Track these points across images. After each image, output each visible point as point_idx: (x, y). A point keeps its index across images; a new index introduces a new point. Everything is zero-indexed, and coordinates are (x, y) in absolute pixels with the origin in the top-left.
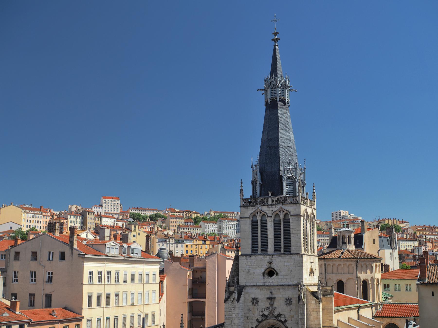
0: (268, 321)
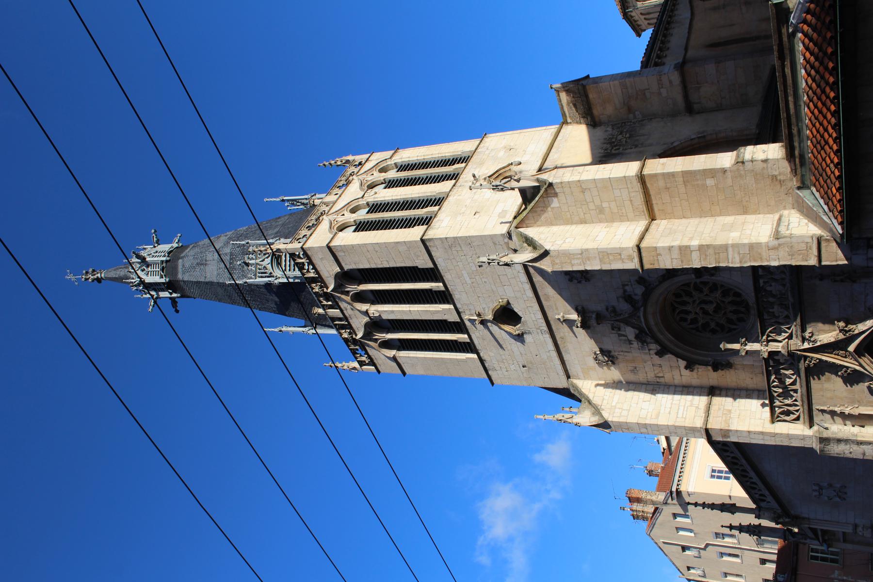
0: (655, 329)
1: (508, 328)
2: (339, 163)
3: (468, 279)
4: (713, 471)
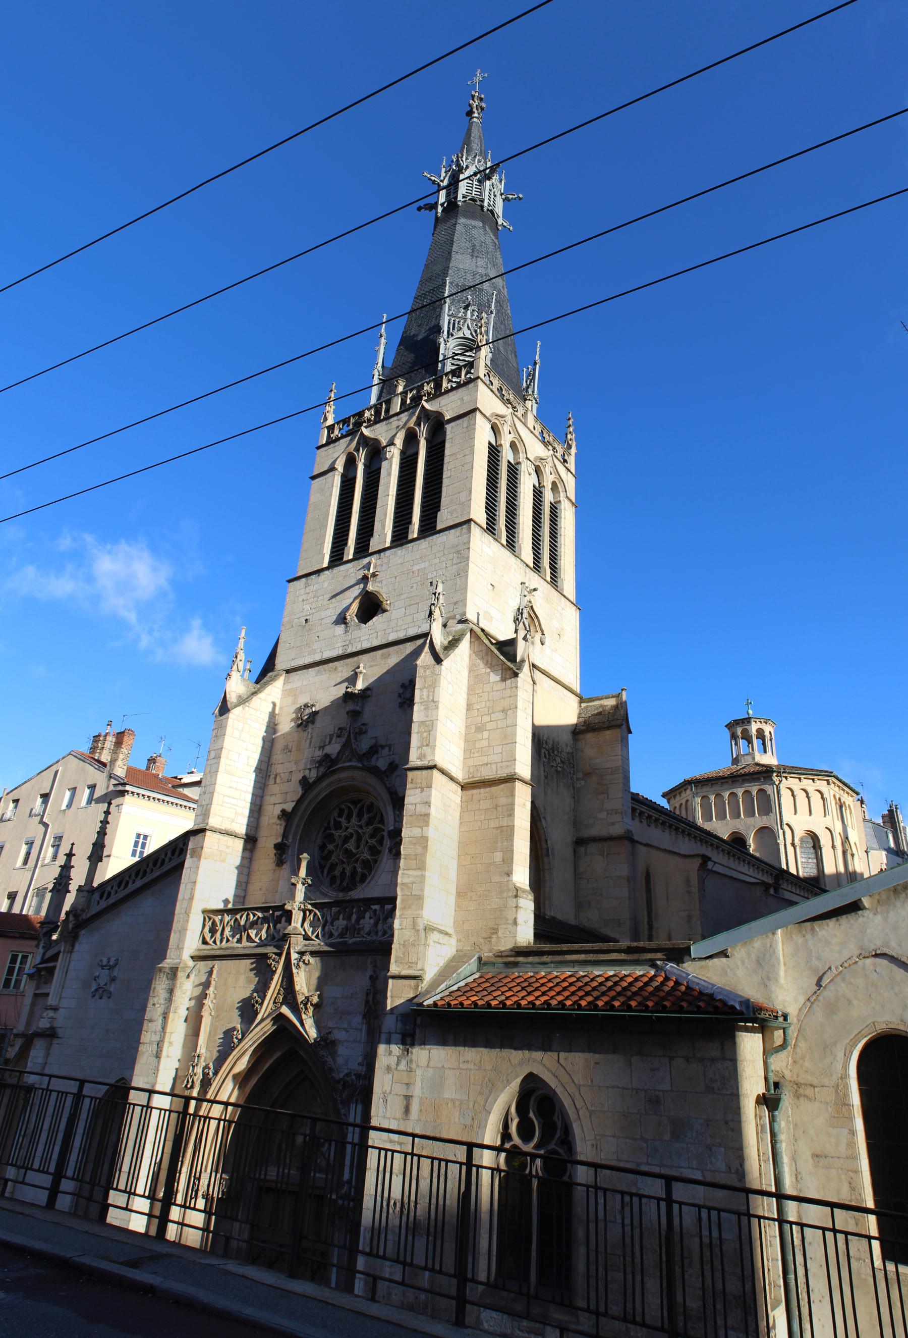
0: (334, 778)
1: (355, 607)
2: (569, 436)
3: (418, 567)
4: (146, 837)
